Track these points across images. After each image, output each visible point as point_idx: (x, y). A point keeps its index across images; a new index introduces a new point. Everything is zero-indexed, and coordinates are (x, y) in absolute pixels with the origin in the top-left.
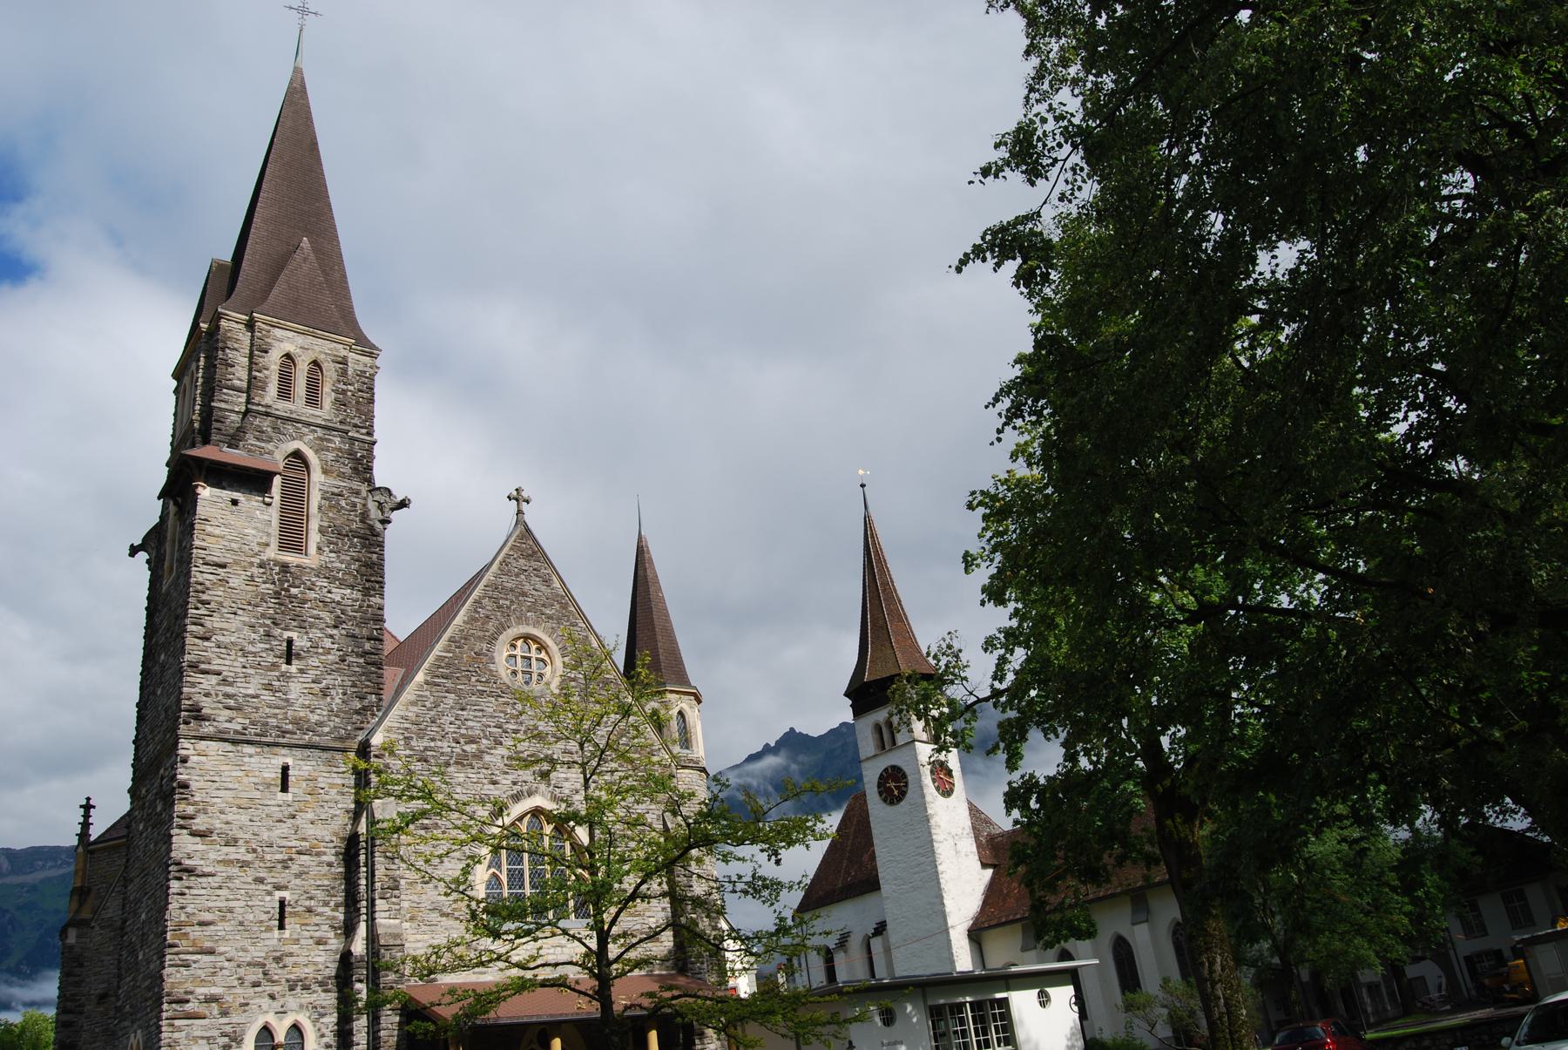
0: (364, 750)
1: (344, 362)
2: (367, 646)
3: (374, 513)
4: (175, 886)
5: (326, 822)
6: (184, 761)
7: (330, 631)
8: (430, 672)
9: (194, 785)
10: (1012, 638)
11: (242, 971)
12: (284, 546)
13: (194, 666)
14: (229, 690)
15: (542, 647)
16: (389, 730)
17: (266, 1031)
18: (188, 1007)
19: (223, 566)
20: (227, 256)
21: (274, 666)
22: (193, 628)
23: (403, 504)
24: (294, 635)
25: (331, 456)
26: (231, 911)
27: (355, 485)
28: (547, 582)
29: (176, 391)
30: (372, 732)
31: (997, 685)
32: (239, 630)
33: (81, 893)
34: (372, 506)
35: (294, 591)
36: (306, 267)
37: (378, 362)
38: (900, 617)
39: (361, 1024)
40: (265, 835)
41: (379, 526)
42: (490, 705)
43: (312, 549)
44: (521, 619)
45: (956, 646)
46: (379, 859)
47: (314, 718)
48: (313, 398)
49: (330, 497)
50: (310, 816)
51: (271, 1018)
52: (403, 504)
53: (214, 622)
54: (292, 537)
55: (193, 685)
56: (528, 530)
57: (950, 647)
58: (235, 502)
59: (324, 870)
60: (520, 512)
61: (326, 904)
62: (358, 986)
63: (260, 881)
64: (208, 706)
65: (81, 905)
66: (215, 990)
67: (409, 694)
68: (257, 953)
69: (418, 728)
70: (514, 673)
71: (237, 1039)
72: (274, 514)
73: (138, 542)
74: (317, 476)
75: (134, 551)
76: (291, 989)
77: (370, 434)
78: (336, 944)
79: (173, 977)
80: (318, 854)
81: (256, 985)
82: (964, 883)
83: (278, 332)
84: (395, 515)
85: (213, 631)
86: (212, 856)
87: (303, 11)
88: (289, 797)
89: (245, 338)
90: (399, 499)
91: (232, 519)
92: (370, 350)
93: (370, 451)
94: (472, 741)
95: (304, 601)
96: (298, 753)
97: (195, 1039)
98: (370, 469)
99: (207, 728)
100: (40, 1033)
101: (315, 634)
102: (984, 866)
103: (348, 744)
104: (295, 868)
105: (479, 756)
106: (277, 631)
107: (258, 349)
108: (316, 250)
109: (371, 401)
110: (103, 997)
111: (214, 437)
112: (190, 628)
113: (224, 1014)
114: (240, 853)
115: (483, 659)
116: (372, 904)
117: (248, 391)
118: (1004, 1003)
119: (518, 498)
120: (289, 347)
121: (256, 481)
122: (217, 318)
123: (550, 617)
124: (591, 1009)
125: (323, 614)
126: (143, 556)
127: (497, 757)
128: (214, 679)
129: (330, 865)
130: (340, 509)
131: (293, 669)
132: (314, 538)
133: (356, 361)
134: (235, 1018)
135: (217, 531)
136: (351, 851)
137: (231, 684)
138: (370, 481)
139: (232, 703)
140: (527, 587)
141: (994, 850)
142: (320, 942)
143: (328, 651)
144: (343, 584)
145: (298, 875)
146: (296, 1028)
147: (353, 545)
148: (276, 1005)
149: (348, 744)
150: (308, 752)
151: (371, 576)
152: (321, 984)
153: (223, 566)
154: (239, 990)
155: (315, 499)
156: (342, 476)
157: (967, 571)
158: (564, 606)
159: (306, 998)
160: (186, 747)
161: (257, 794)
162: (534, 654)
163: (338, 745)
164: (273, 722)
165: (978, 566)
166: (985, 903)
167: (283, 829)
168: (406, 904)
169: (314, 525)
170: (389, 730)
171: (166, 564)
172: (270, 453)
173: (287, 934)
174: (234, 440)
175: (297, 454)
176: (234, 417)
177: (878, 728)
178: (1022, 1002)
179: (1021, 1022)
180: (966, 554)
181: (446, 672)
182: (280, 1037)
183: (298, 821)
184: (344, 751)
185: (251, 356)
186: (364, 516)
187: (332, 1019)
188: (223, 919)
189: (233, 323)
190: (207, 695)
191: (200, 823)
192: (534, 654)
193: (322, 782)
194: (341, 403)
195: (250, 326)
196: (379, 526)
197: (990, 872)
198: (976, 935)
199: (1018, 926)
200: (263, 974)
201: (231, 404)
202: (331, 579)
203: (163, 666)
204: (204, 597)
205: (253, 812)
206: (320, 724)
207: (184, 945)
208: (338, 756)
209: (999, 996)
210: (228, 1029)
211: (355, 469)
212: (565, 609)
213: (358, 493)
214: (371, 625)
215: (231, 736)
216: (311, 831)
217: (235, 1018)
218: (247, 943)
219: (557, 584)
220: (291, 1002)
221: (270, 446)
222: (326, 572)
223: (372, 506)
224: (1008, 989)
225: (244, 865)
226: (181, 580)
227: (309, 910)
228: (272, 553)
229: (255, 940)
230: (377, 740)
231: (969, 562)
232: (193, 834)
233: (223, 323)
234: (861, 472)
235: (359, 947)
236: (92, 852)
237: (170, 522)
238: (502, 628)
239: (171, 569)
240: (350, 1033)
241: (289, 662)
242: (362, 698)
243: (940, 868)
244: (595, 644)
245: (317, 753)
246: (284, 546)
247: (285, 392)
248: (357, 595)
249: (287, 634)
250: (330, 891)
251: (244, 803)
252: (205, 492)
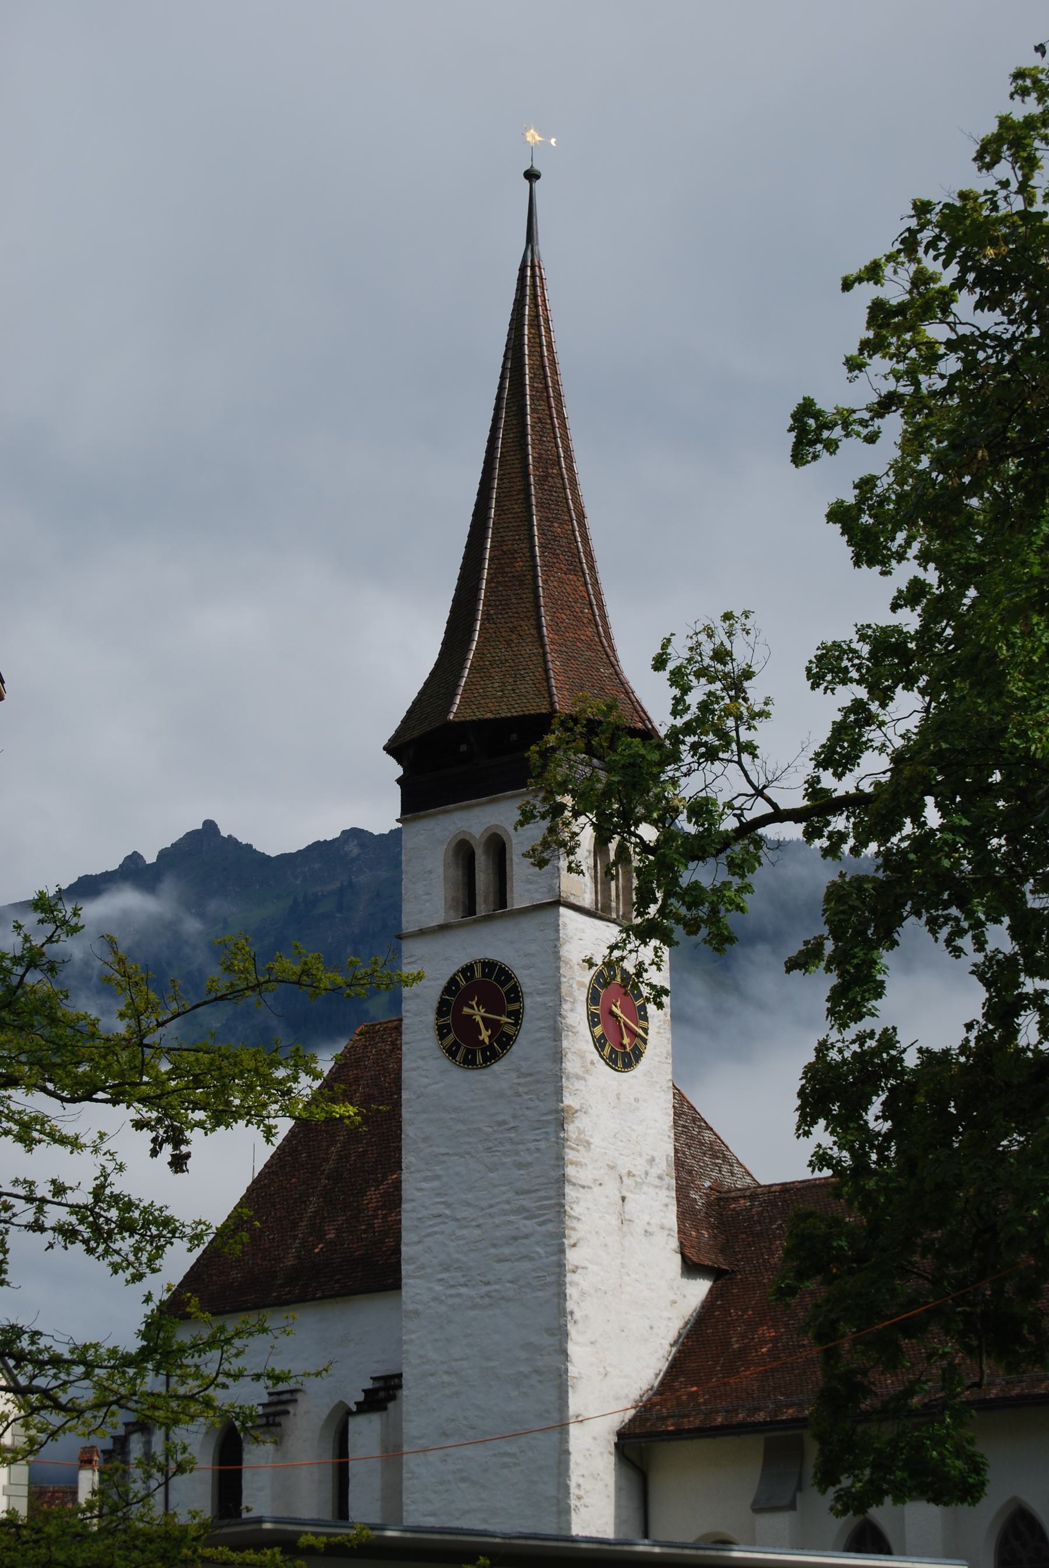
10: (887, 660)
31: (827, 780)
38: (575, 560)
45: (741, 654)
57: (721, 655)
82: (628, 1307)
102: (691, 1268)
141: (726, 1227)
157: (798, 458)
165: (832, 446)
177: (464, 853)
180: (806, 409)
197: (700, 1288)
198: (638, 1447)
199: (754, 1445)
231: (810, 432)
234: (533, 136)
243: (572, 1257)
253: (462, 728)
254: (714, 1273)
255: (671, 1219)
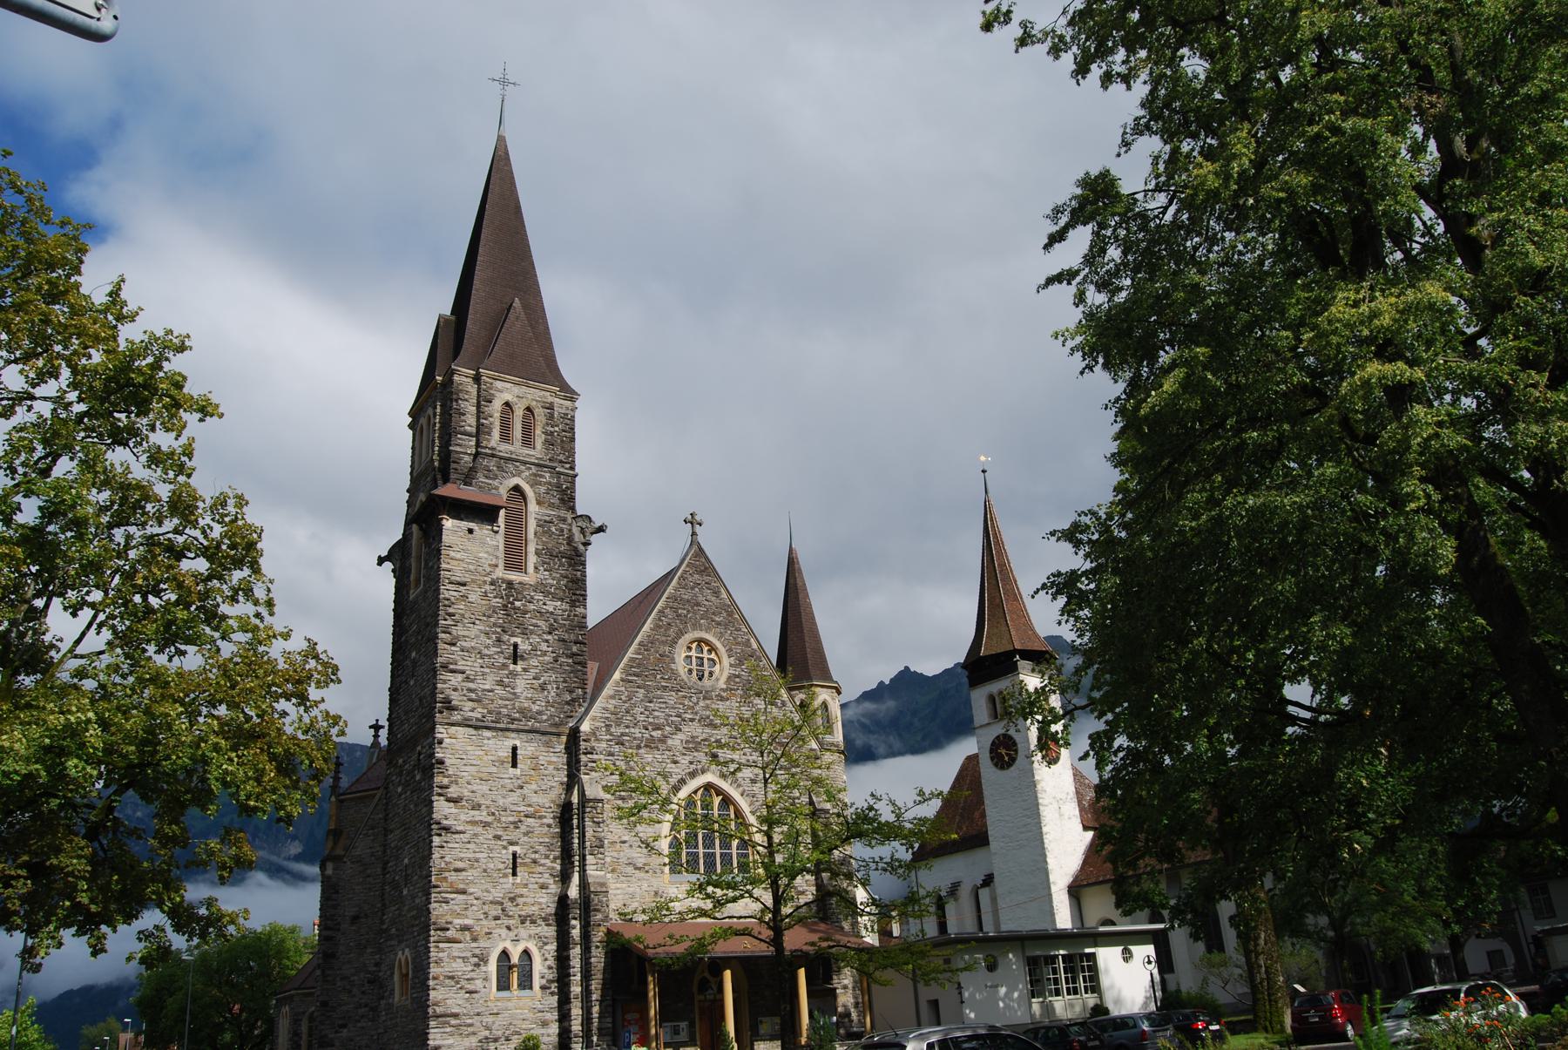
0: (574, 735)
1: (551, 407)
2: (575, 649)
3: (578, 537)
4: (436, 840)
5: (546, 793)
6: (440, 742)
7: (546, 637)
8: (626, 672)
9: (448, 762)
11: (486, 908)
12: (509, 566)
13: (444, 667)
14: (471, 685)
15: (712, 649)
16: (594, 719)
17: (505, 954)
18: (449, 934)
19: (464, 584)
20: (447, 310)
21: (504, 666)
22: (441, 635)
23: (601, 529)
24: (518, 640)
25: (543, 489)
26: (477, 860)
27: (563, 513)
28: (716, 593)
29: (411, 426)
30: (581, 720)
32: (477, 637)
33: (336, 834)
34: (576, 530)
35: (517, 604)
36: (518, 324)
37: (577, 404)
39: (576, 952)
40: (501, 802)
41: (581, 547)
42: (671, 698)
43: (531, 569)
44: (696, 626)
46: (588, 823)
47: (535, 708)
48: (528, 440)
49: (543, 524)
50: (534, 787)
51: (508, 945)
52: (601, 529)
53: (459, 631)
54: (514, 560)
55: (445, 682)
56: (701, 549)
58: (470, 531)
59: (544, 830)
60: (694, 534)
61: (547, 857)
62: (573, 922)
63: (498, 837)
64: (456, 699)
65: (335, 844)
66: (468, 922)
67: (608, 690)
68: (497, 894)
69: (615, 718)
70: (690, 671)
71: (483, 959)
72: (500, 540)
73: (384, 554)
74: (533, 507)
75: (381, 561)
76: (523, 922)
77: (572, 468)
78: (555, 888)
79: (438, 911)
80: (540, 817)
81: (497, 918)
82: (1066, 842)
83: (499, 384)
84: (594, 538)
85: (458, 638)
86: (463, 817)
87: (504, 82)
88: (518, 772)
89: (473, 389)
90: (597, 525)
91: (469, 546)
92: (570, 394)
93: (573, 483)
94: (657, 728)
95: (526, 612)
96: (524, 736)
97: (454, 958)
98: (572, 499)
99: (456, 717)
100: (283, 941)
101: (535, 639)
102: (1086, 828)
103: (561, 729)
104: (523, 828)
105: (663, 740)
106: (505, 638)
107: (483, 400)
108: (525, 306)
109: (573, 439)
110: (355, 919)
111: (453, 476)
112: (441, 635)
113: (475, 940)
114: (482, 815)
115: (666, 659)
116: (583, 858)
117: (477, 435)
118: (1092, 957)
119: (692, 521)
120: (508, 397)
121: (485, 513)
122: (450, 374)
123: (719, 624)
124: (764, 949)
125: (540, 623)
126: (388, 566)
127: (676, 741)
128: (460, 677)
129: (549, 826)
130: (549, 533)
131: (519, 668)
132: (532, 559)
133: (561, 404)
134: (482, 944)
135: (458, 556)
136: (565, 815)
137: (472, 681)
138: (573, 509)
139: (473, 696)
140: (701, 598)
142: (543, 887)
143: (544, 653)
144: (555, 597)
145: (526, 834)
146: (526, 953)
147: (562, 565)
148: (512, 934)
149: (561, 729)
150: (531, 736)
151: (576, 589)
152: (545, 919)
153: (464, 584)
154: (484, 922)
155: (532, 526)
156: (551, 506)
158: (730, 614)
159: (534, 930)
160: (441, 732)
161: (494, 769)
162: (705, 655)
163: (554, 730)
164: (505, 711)
166: (1085, 863)
167: (514, 797)
168: (608, 859)
169: (532, 548)
170: (594, 719)
171: (412, 577)
172: (497, 488)
173: (518, 880)
174: (468, 479)
175: (517, 488)
176: (467, 458)
177: (992, 699)
178: (1107, 957)
179: (1107, 971)
181: (638, 671)
182: (515, 959)
183: (525, 791)
184: (559, 735)
185: (478, 406)
186: (570, 540)
187: (552, 947)
188: (472, 867)
189: (463, 377)
190: (455, 690)
191: (453, 791)
192: (705, 655)
193: (542, 759)
194: (549, 443)
195: (477, 379)
196: (581, 547)
197: (1090, 834)
198: (1075, 891)
200: (502, 909)
201: (464, 447)
202: (546, 593)
203: (414, 662)
204: (451, 610)
205: (488, 782)
206: (540, 713)
207: (444, 886)
208: (554, 739)
209: (1088, 950)
210: (477, 951)
211: (562, 500)
212: (731, 617)
213: (564, 520)
214: (577, 631)
215: (473, 722)
216: (535, 799)
217: (482, 944)
218: (489, 886)
219: (724, 595)
220: (523, 932)
221: (496, 483)
222: (541, 587)
223: (576, 530)
224: (1096, 946)
225: (486, 825)
226: (430, 594)
227: (535, 862)
228: (500, 573)
229: (495, 884)
230: (585, 727)
232: (449, 800)
233: (456, 378)
234: (983, 458)
235: (573, 892)
236: (342, 801)
237: (414, 542)
238: (681, 633)
239: (418, 582)
240: (568, 958)
241: (515, 663)
242: (571, 692)
243: (1045, 830)
244: (755, 646)
245: (538, 736)
246: (509, 566)
247: (506, 436)
248: (565, 606)
249: (513, 640)
250: (549, 847)
251: (484, 776)
252: (449, 523)
253: (985, 657)
254: (1094, 829)
255: (1077, 812)
